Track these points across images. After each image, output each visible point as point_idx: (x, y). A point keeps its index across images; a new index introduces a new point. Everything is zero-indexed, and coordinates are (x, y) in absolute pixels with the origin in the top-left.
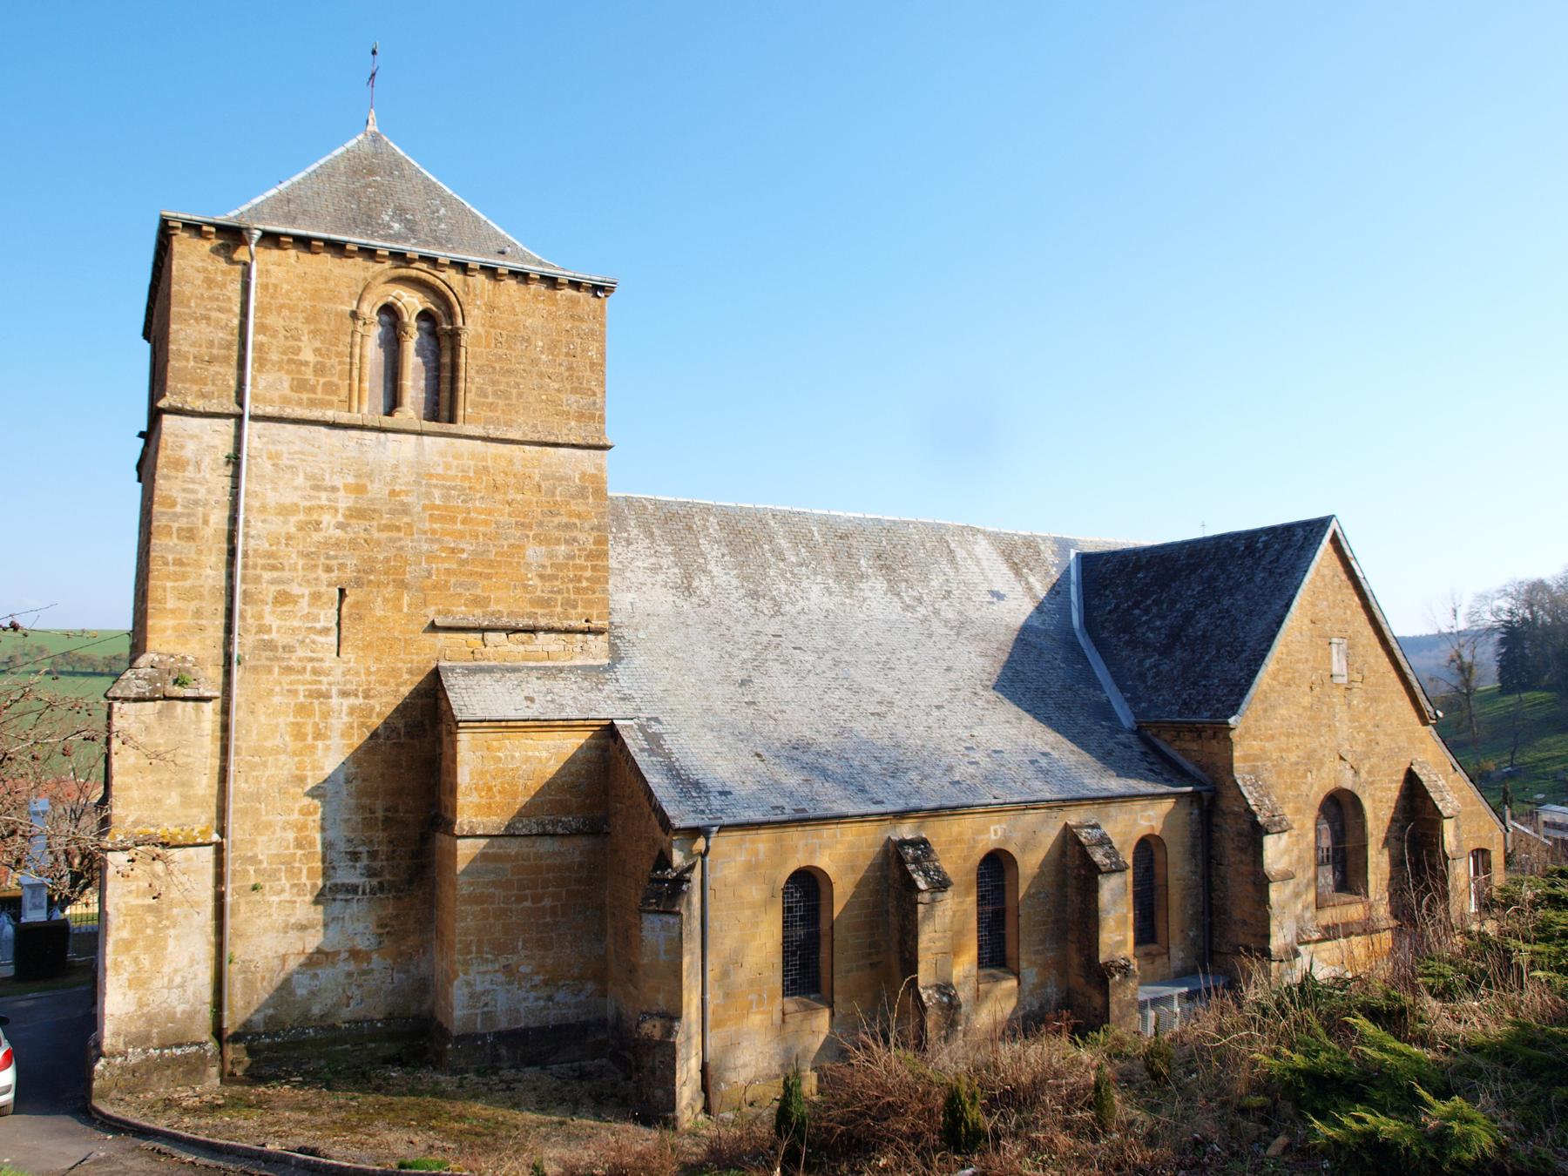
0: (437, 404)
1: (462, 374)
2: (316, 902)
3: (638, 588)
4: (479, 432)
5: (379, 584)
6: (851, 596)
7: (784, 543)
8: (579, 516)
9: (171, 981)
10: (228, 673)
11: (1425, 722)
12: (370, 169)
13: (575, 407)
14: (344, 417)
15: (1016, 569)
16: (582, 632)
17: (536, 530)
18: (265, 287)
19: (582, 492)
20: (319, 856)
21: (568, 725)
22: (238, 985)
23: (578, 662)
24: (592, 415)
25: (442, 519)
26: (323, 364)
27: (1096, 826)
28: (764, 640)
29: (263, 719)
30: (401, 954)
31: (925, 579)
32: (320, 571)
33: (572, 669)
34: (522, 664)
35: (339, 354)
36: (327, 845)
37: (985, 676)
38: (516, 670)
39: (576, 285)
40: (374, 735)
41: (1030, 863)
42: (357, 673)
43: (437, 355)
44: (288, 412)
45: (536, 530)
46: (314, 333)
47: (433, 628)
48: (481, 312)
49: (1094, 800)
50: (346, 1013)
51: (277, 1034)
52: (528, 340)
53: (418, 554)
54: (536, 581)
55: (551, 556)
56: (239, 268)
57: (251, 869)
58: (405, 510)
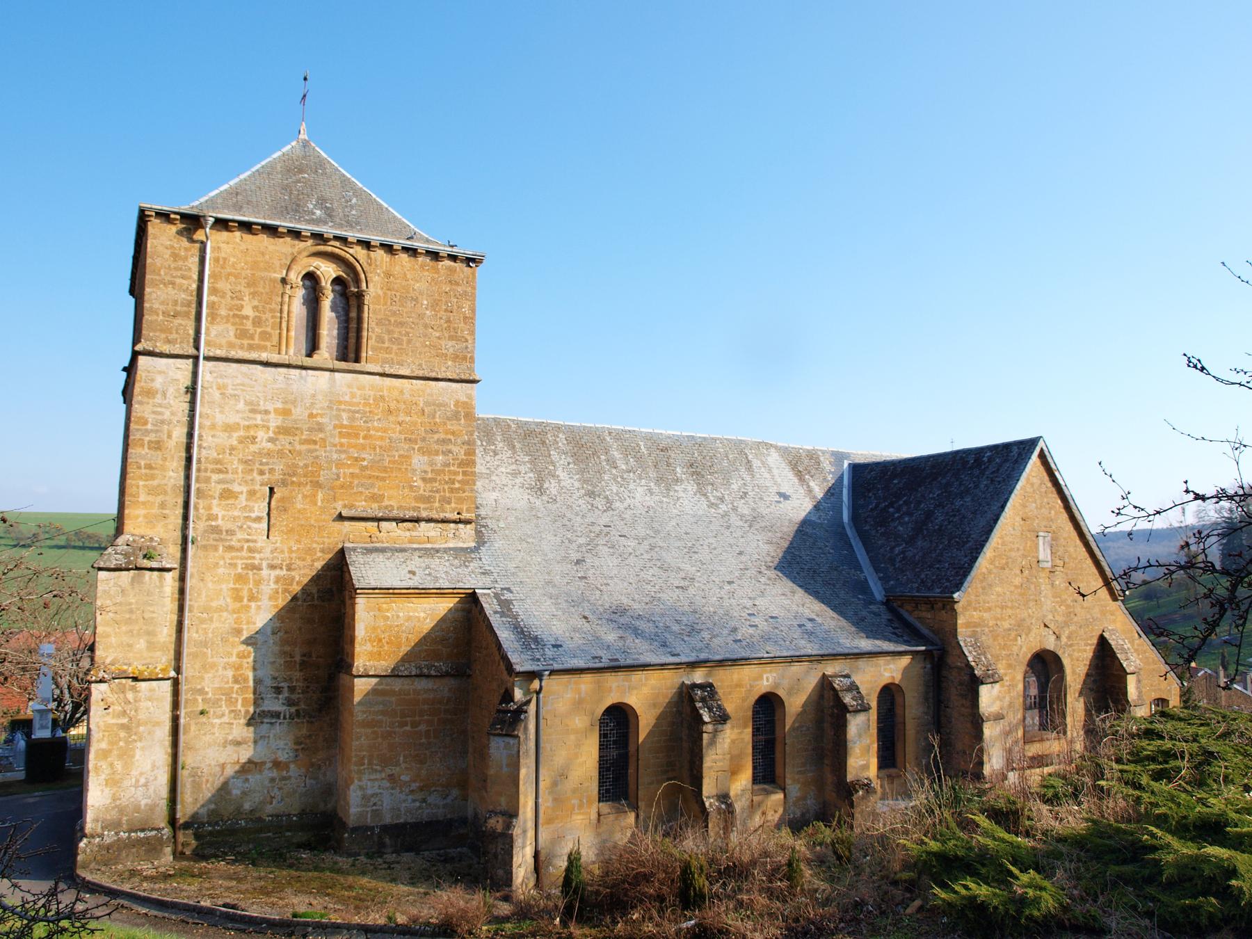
0: (346, 347)
1: (365, 326)
2: (248, 724)
3: (501, 487)
4: (378, 369)
5: (300, 484)
6: (667, 496)
7: (617, 454)
8: (453, 433)
9: (137, 781)
10: (184, 551)
11: (1115, 599)
12: (302, 168)
13: (451, 350)
14: (275, 358)
15: (800, 476)
16: (455, 522)
17: (420, 444)
18: (217, 260)
19: (456, 416)
20: (251, 690)
21: (441, 593)
22: (188, 786)
23: (451, 545)
24: (465, 357)
25: (348, 435)
26: (260, 318)
27: (847, 676)
28: (597, 529)
29: (210, 585)
30: (312, 765)
31: (728, 483)
32: (255, 474)
33: (446, 550)
34: (408, 546)
35: (272, 310)
36: (258, 681)
37: (769, 559)
38: (403, 550)
39: (453, 258)
40: (295, 598)
41: (795, 704)
42: (282, 552)
43: (347, 311)
44: (233, 354)
45: (420, 444)
46: (253, 294)
47: (340, 518)
48: (379, 277)
49: (846, 656)
50: (269, 809)
51: (217, 823)
52: (416, 300)
53: (330, 462)
54: (419, 483)
55: (432, 464)
56: (198, 245)
57: (200, 698)
58: (320, 428)
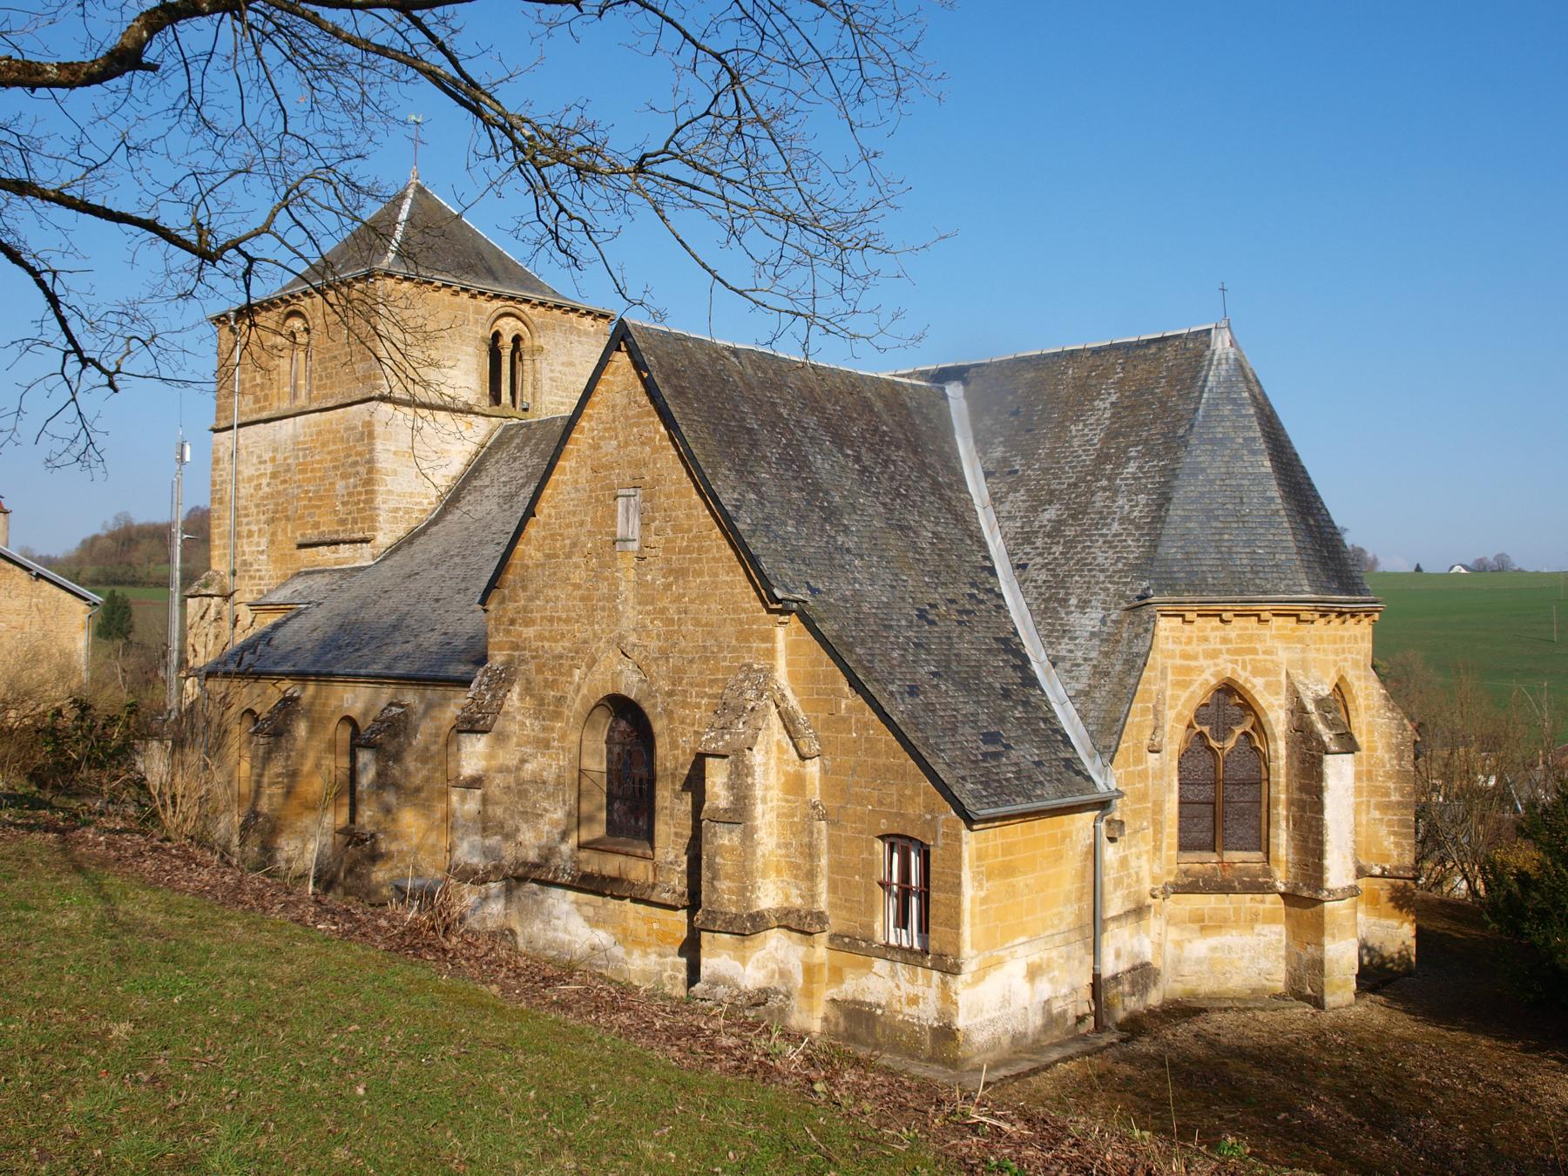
47: (301, 546)
